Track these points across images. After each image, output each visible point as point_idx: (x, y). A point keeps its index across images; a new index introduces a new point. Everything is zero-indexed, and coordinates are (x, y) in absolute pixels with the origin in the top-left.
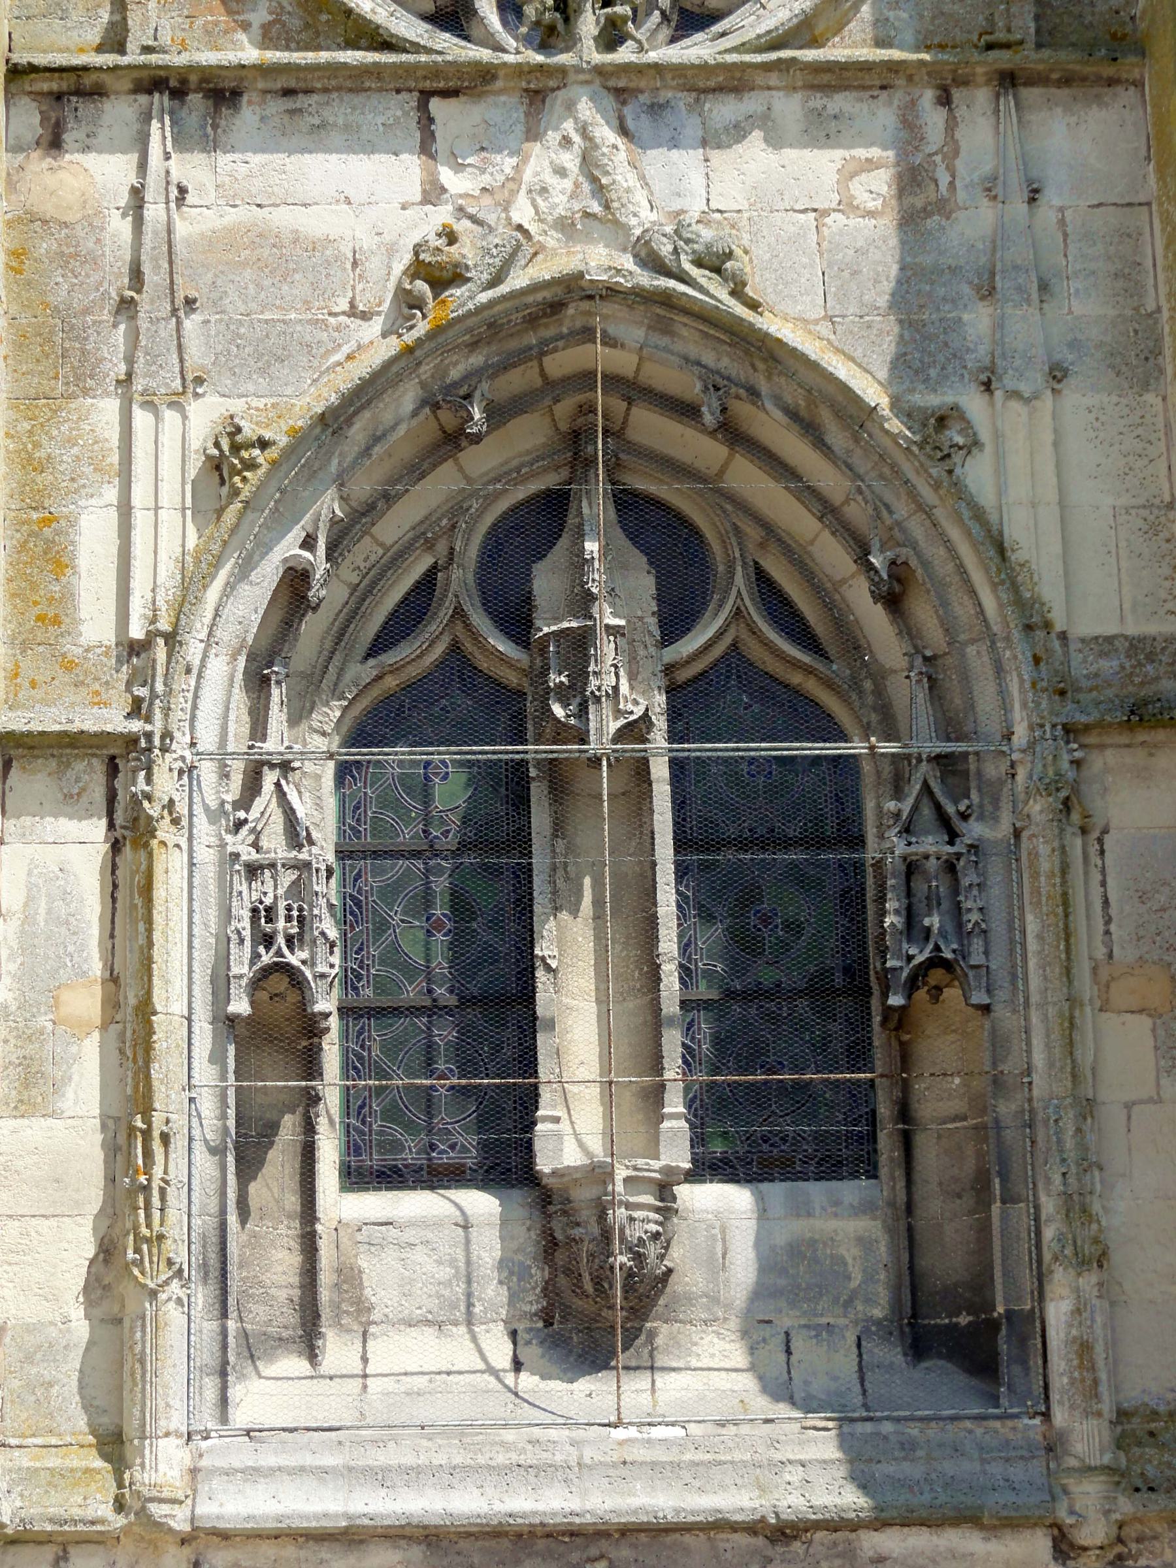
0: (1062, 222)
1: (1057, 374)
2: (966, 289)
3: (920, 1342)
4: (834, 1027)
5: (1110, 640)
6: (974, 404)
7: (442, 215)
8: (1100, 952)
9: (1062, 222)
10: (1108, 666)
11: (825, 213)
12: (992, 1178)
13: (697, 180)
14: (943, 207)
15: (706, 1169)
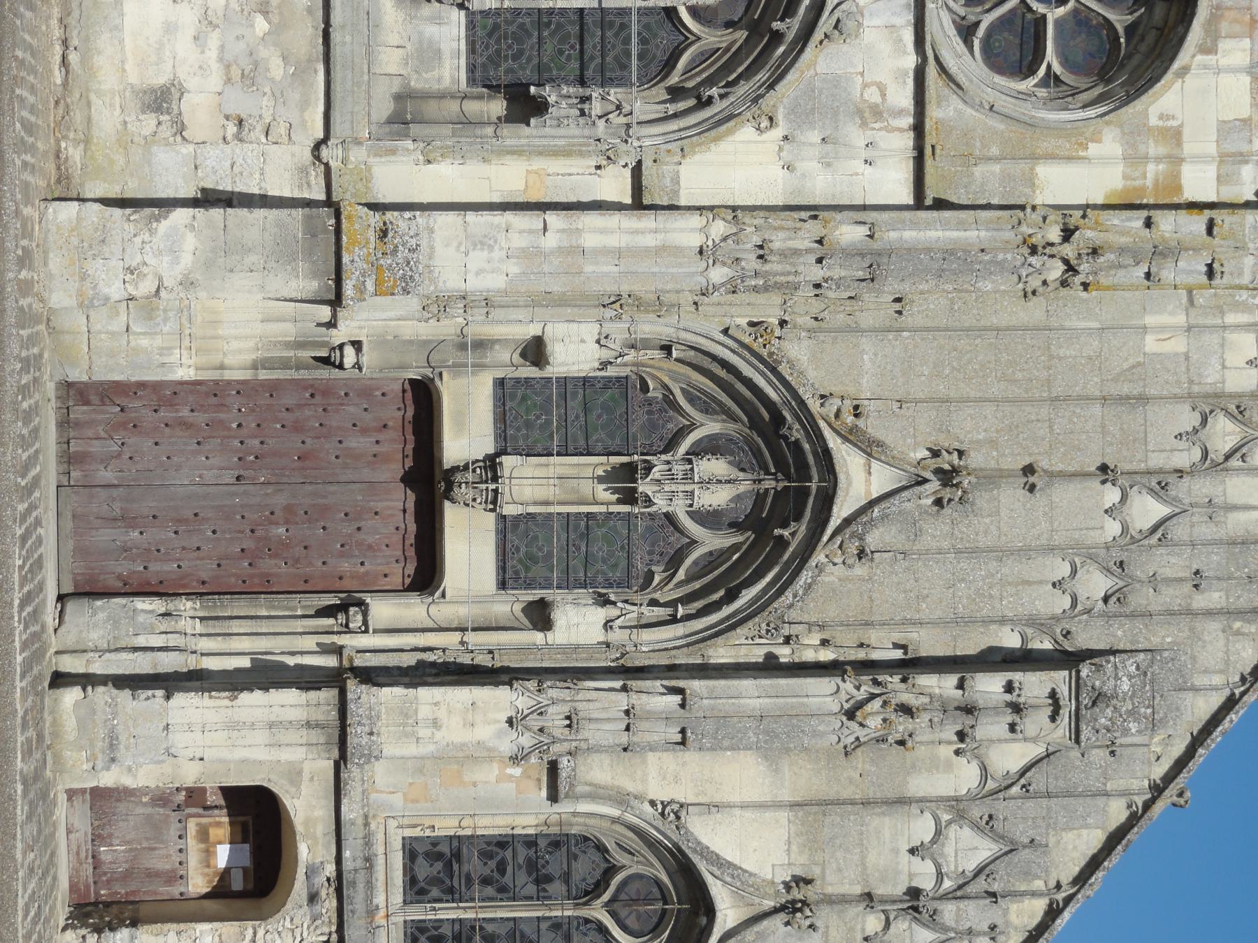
0: (857, 174)
1: (789, 167)
2: (828, 133)
3: (399, 98)
4: (528, 72)
5: (678, 183)
6: (777, 133)
8: (550, 171)
9: (857, 174)
10: (668, 182)
11: (862, 74)
13: (877, 22)
14: (864, 124)
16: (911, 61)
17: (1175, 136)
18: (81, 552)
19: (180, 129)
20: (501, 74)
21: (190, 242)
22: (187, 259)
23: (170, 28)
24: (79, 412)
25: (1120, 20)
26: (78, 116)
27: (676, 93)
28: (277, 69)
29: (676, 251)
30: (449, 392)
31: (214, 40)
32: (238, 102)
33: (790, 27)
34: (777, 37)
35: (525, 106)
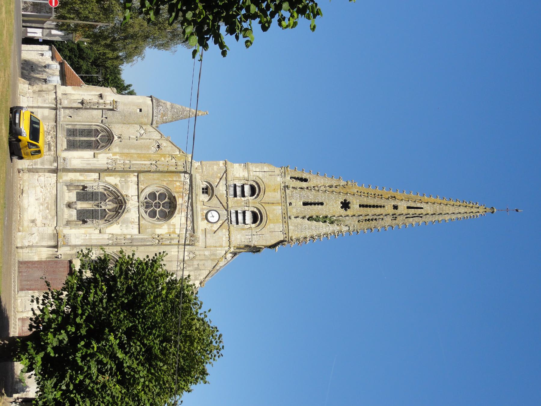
3: (67, 221)
6: (120, 225)
7: (130, 196)
12: (76, 225)
15: (77, 211)
16: (138, 215)
17: (174, 225)
18: (21, 285)
19: (36, 225)
20: (81, 218)
21: (37, 238)
22: (37, 240)
23: (35, 212)
24: (21, 265)
25: (167, 211)
26: (21, 223)
27: (106, 220)
28: (50, 217)
29: (105, 239)
30: (74, 262)
31: (41, 213)
32: (44, 222)
33: (121, 211)
34: (119, 213)
35: (84, 222)
